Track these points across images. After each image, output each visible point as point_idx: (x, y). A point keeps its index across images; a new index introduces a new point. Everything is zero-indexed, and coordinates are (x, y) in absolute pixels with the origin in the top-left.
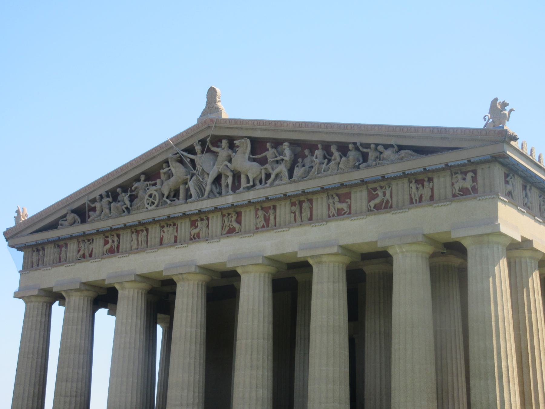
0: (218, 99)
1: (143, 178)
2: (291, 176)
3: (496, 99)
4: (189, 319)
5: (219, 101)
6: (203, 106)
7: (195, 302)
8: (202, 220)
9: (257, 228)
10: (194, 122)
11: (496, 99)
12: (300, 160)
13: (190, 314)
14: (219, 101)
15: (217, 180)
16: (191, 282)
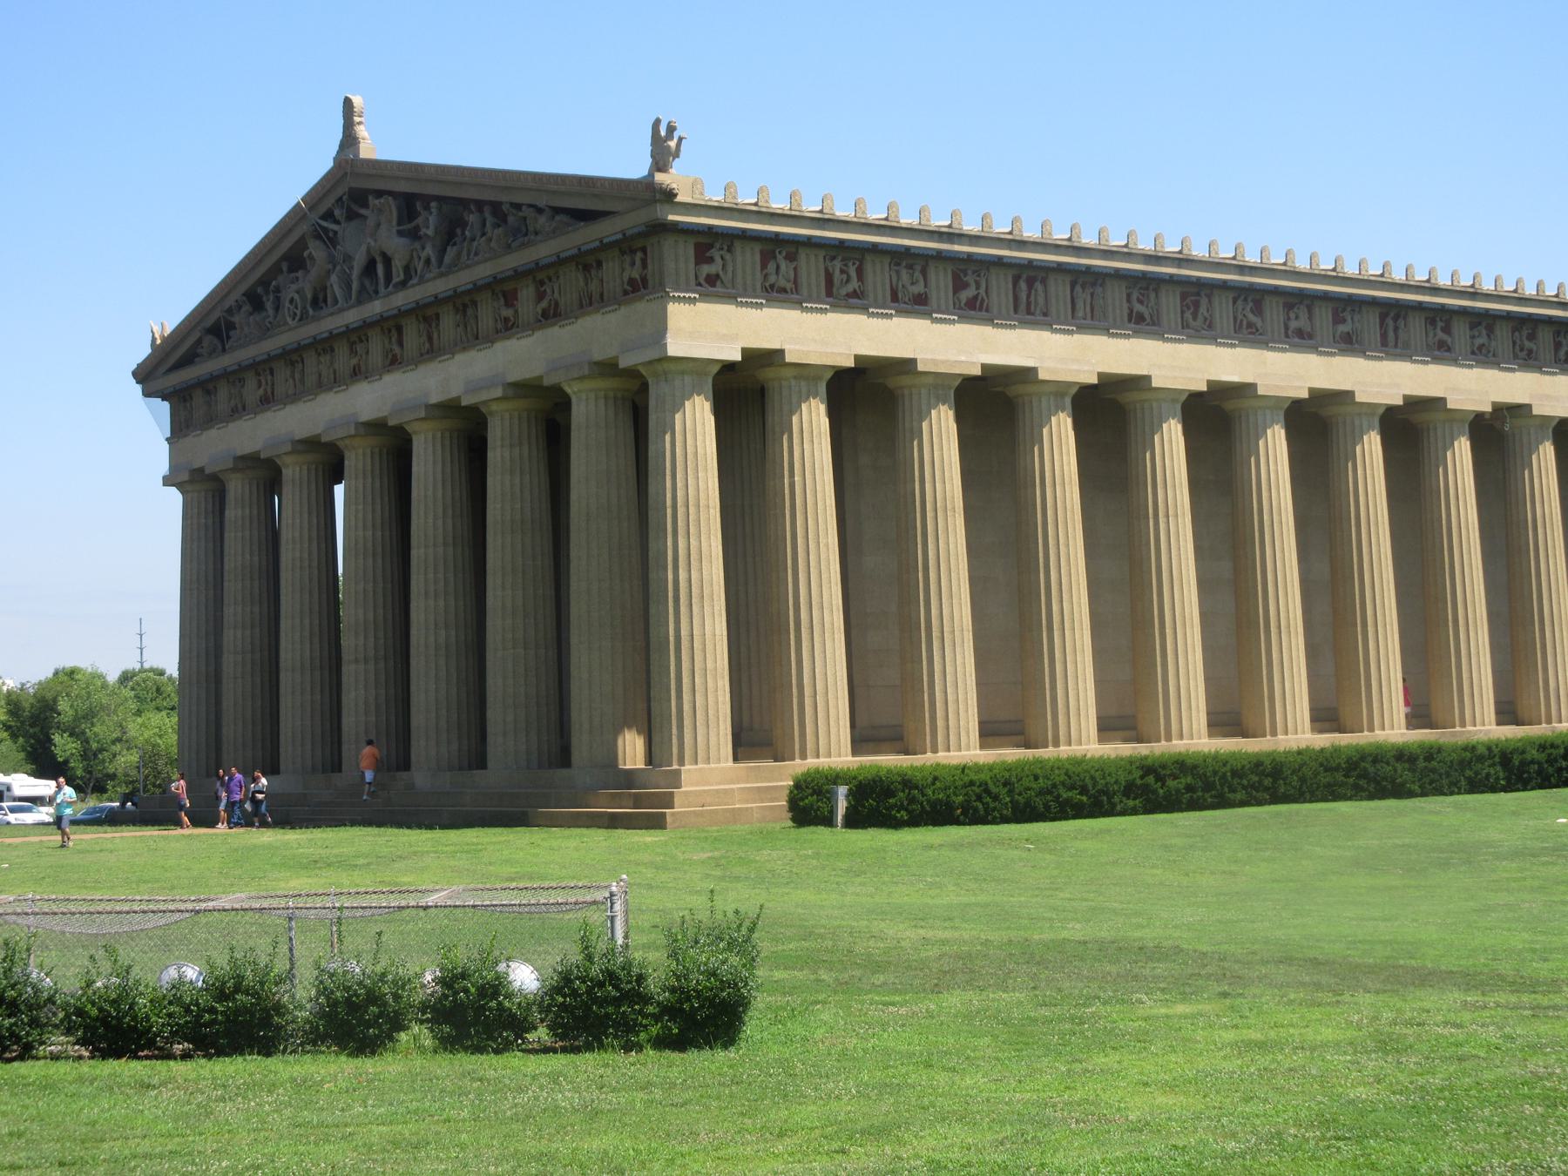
0: (357, 119)
1: (285, 266)
2: (440, 262)
3: (657, 122)
4: (360, 515)
5: (360, 123)
6: (338, 135)
7: (369, 485)
8: (361, 341)
9: (422, 355)
10: (330, 164)
11: (657, 122)
12: (459, 231)
13: (361, 507)
14: (360, 123)
15: (370, 268)
16: (361, 451)
